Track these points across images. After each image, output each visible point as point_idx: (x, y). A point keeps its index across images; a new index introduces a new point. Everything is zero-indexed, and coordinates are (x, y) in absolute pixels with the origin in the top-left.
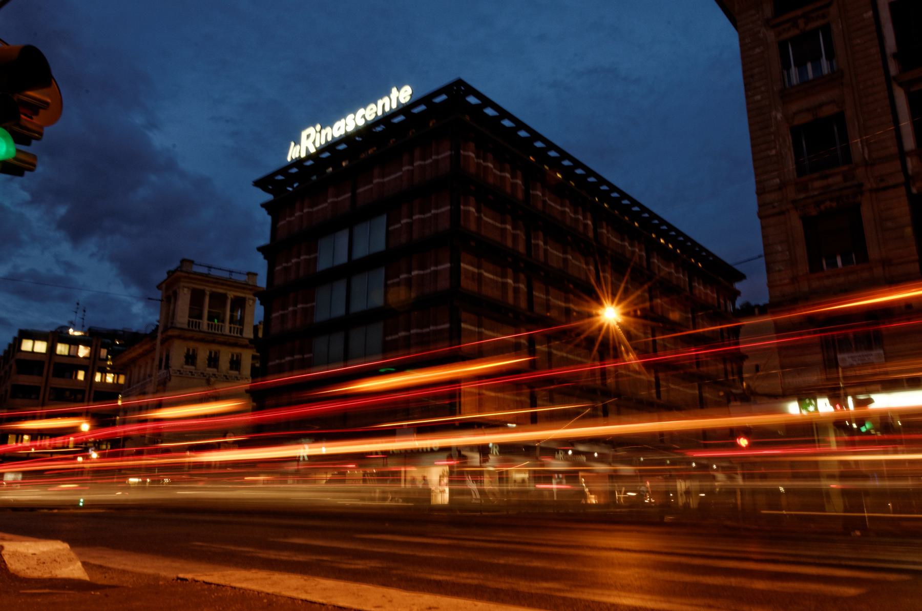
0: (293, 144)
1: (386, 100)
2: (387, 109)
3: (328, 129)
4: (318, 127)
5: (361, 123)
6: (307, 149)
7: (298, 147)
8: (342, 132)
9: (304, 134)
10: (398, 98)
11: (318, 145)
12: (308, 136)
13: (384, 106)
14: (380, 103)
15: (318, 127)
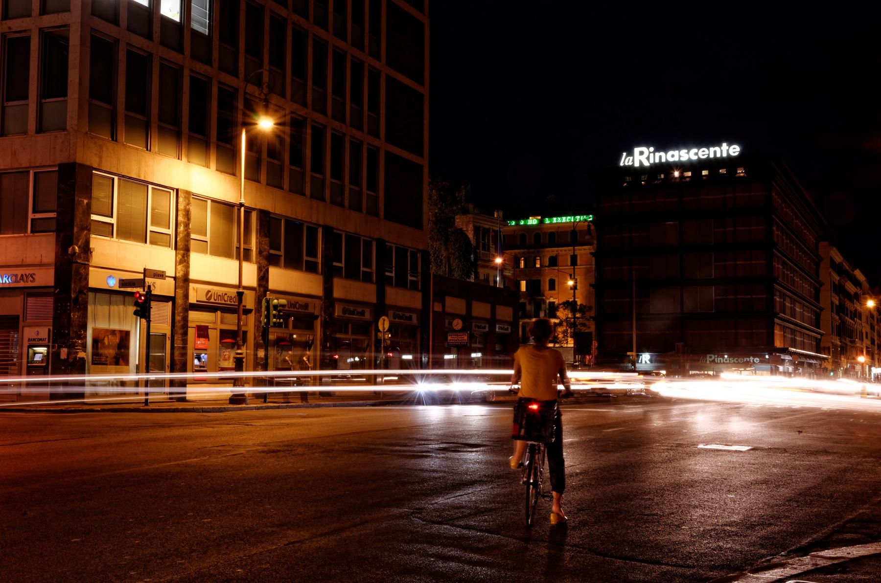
0: (625, 154)
1: (717, 149)
2: (718, 155)
3: (662, 154)
4: (652, 149)
5: (694, 158)
6: (641, 162)
7: (631, 158)
8: (676, 159)
9: (637, 150)
10: (728, 151)
11: (652, 161)
12: (641, 153)
13: (715, 152)
14: (712, 149)
15: (652, 149)
